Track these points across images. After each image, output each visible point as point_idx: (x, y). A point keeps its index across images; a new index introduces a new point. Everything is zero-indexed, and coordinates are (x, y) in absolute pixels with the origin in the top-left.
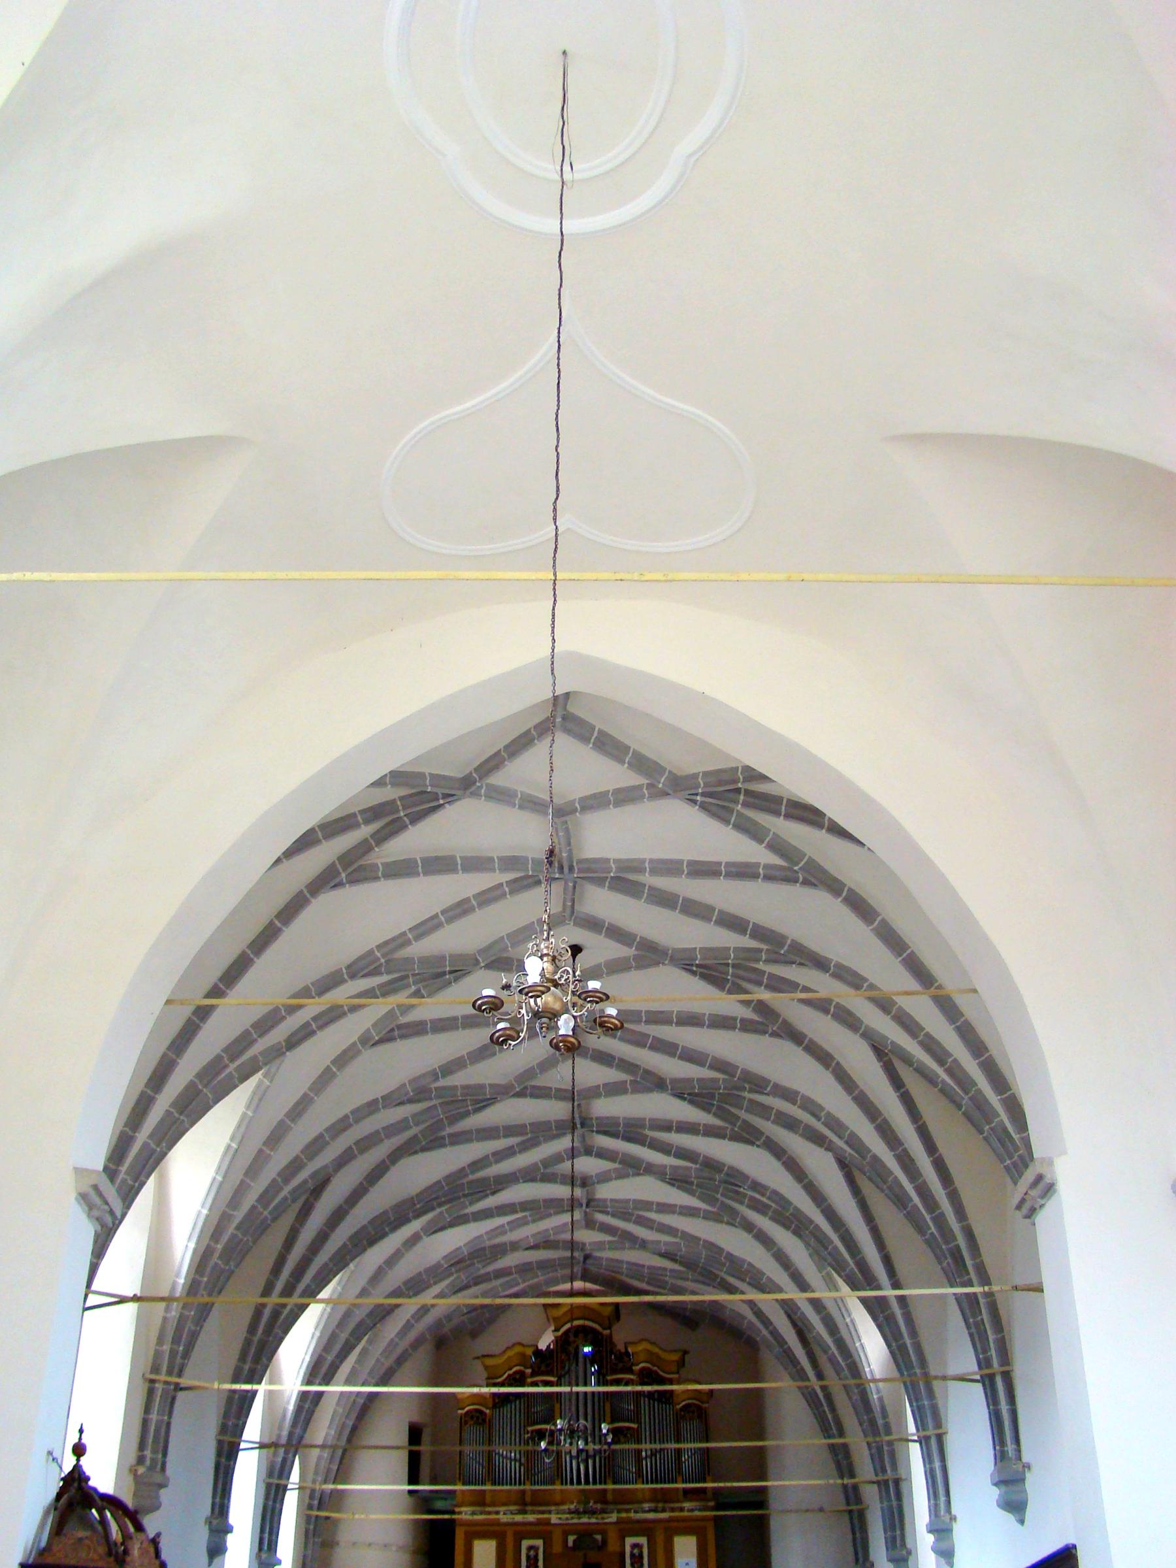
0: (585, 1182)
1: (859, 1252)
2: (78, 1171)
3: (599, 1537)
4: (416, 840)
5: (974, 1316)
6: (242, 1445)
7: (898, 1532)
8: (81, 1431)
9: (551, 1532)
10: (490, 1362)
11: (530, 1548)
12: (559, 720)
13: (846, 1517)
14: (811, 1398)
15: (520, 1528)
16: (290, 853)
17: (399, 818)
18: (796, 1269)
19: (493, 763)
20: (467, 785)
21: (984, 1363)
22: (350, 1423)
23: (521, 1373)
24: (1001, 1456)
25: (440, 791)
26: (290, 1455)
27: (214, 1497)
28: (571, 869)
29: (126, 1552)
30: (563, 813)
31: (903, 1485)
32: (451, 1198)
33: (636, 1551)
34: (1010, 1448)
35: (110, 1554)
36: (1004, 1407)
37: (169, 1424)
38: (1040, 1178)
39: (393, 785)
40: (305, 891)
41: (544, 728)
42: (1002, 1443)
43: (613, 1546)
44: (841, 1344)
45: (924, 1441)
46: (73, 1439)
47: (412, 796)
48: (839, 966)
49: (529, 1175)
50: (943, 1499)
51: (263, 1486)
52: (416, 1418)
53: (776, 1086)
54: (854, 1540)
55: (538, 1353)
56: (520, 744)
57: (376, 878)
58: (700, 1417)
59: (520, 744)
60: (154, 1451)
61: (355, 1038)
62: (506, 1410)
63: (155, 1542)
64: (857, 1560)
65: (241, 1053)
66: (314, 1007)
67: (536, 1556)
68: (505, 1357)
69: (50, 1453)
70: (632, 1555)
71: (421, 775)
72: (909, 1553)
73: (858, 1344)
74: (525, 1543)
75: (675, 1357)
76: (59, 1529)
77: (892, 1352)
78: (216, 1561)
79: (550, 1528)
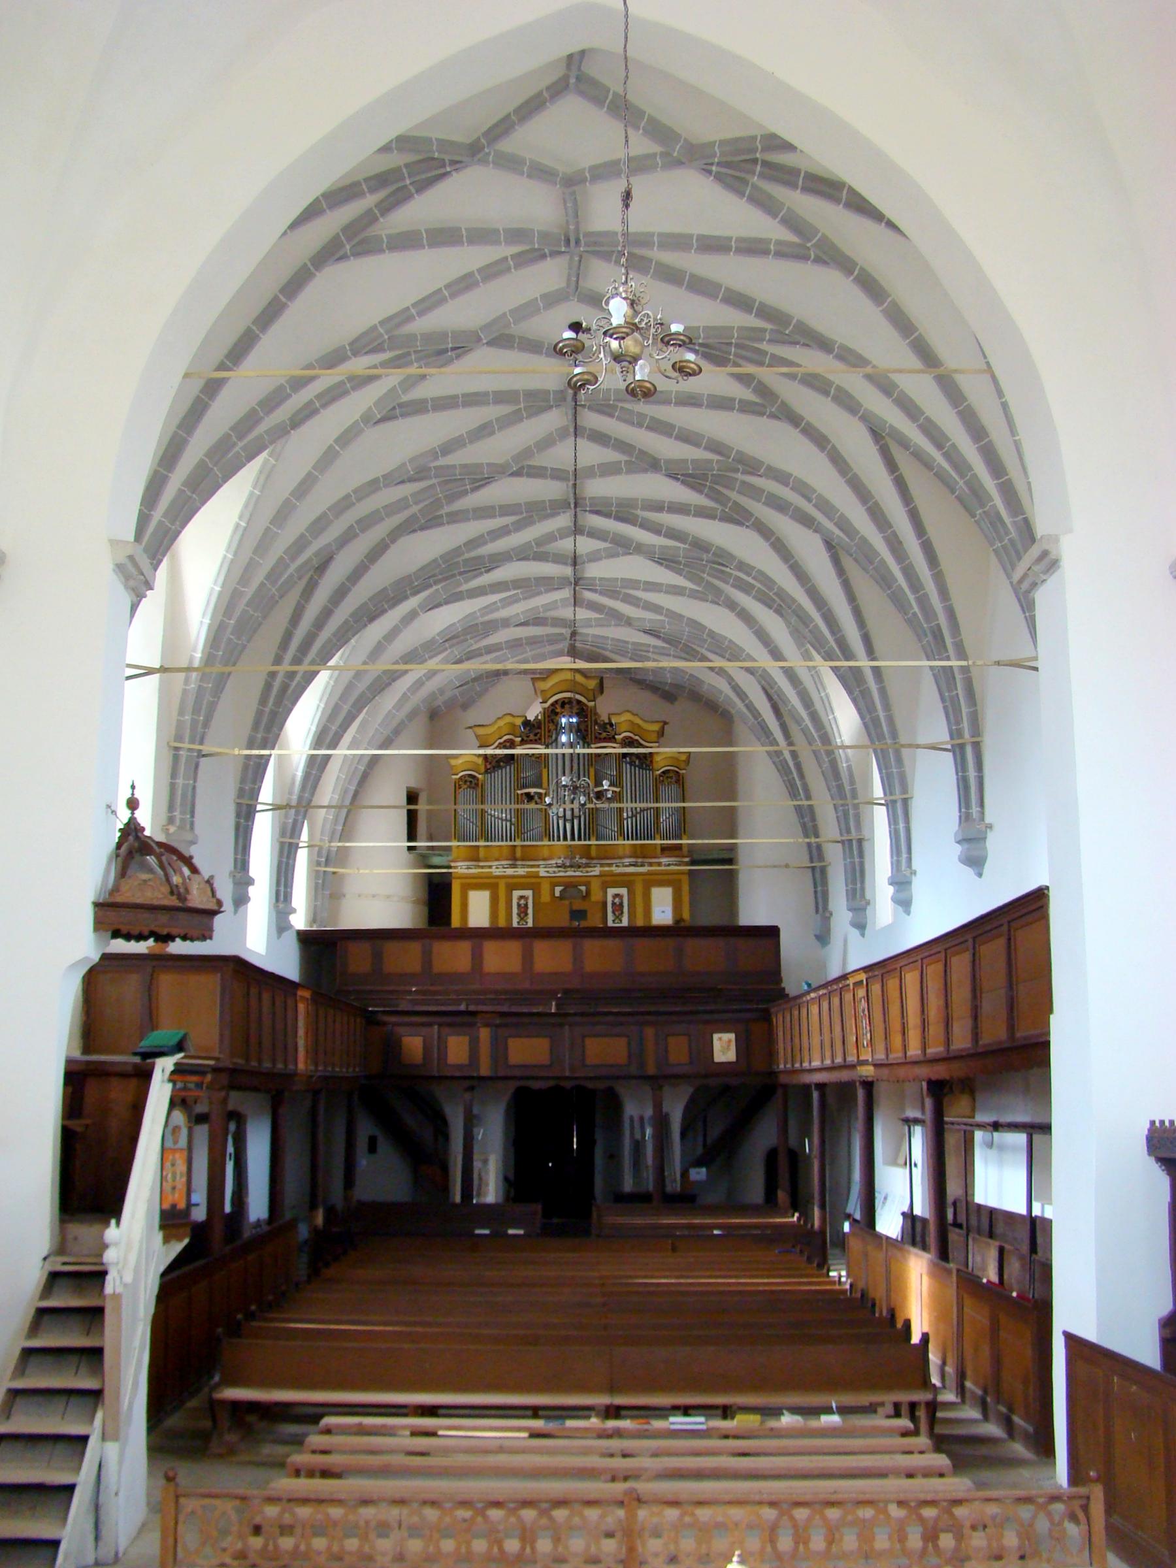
0: (575, 561)
1: (840, 630)
2: (114, 543)
3: (583, 888)
4: (423, 210)
5: (950, 691)
6: (259, 807)
7: (859, 885)
8: (133, 787)
9: (539, 884)
10: (481, 731)
11: (521, 897)
12: (572, 81)
13: (809, 871)
14: (782, 768)
15: (510, 881)
16: (295, 225)
17: (405, 186)
18: (776, 647)
19: (503, 128)
20: (474, 151)
21: (955, 733)
22: (353, 788)
24: (965, 817)
25: (447, 158)
26: (300, 818)
27: (236, 853)
28: (577, 242)
29: (187, 891)
30: (572, 184)
31: (866, 845)
32: (447, 576)
33: (617, 900)
34: (975, 809)
35: (172, 893)
36: (972, 774)
37: (194, 788)
38: (1045, 554)
39: (400, 150)
40: (309, 264)
41: (558, 90)
42: (968, 806)
43: (596, 896)
44: (815, 717)
45: (890, 805)
46: (124, 794)
47: (418, 164)
48: (843, 348)
49: (523, 554)
50: (904, 856)
51: (277, 846)
52: (413, 784)
53: (769, 468)
54: (816, 892)
55: (526, 723)
56: (531, 107)
57: (381, 251)
58: (677, 782)
59: (531, 107)
60: (183, 813)
61: (357, 417)
62: (498, 774)
63: (209, 882)
64: (817, 911)
65: (250, 429)
66: (328, 379)
67: (526, 905)
68: (496, 727)
69: (109, 807)
70: (614, 904)
71: (429, 140)
72: (868, 903)
73: (831, 717)
74: (516, 894)
75: (656, 727)
76: (123, 873)
77: (865, 725)
78: (242, 909)
79: (538, 880)
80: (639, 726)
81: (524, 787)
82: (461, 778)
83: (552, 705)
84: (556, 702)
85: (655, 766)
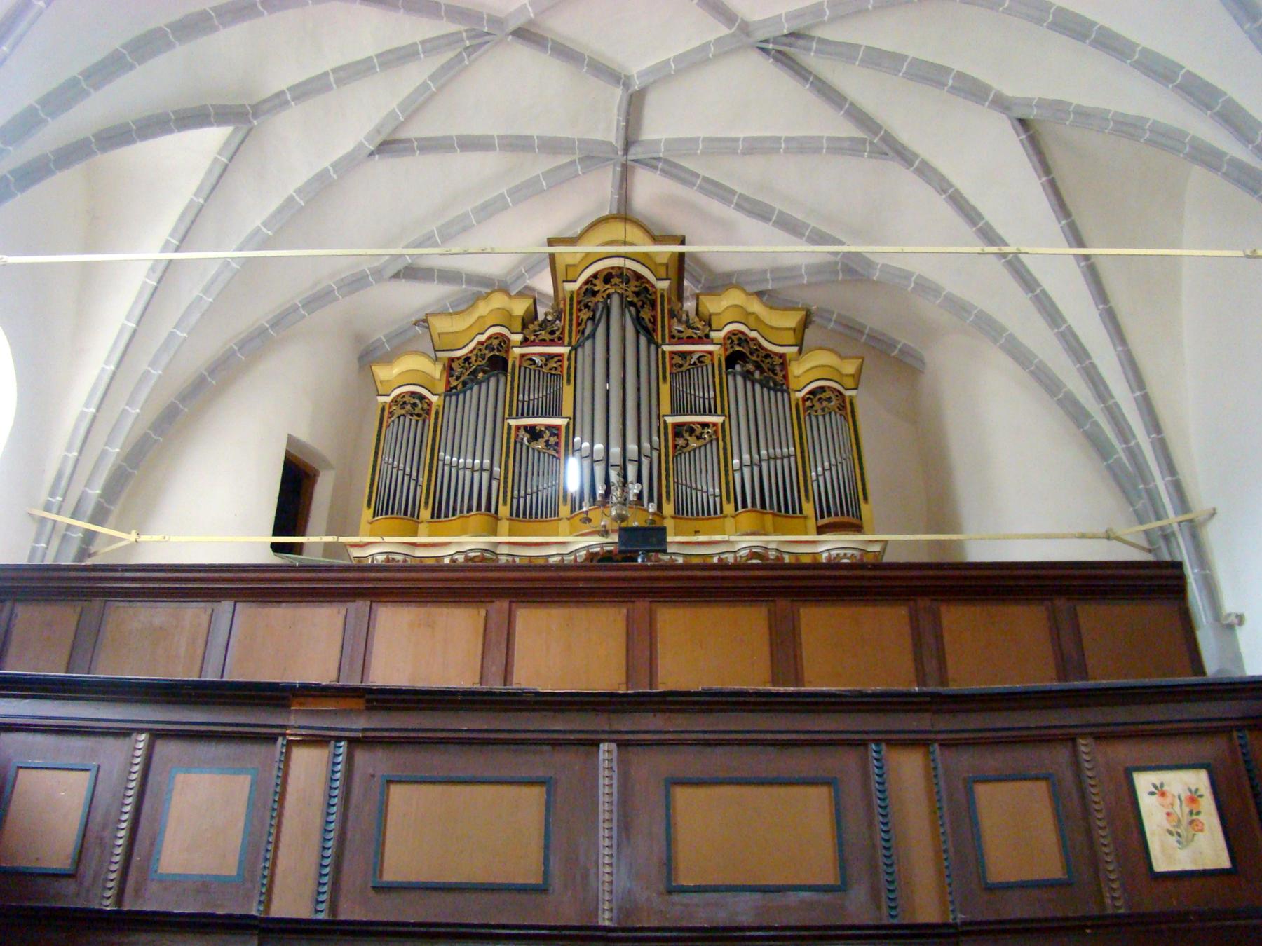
23: (503, 342)
80: (758, 318)
81: (522, 415)
82: (395, 401)
83: (587, 282)
84: (595, 276)
85: (793, 384)
